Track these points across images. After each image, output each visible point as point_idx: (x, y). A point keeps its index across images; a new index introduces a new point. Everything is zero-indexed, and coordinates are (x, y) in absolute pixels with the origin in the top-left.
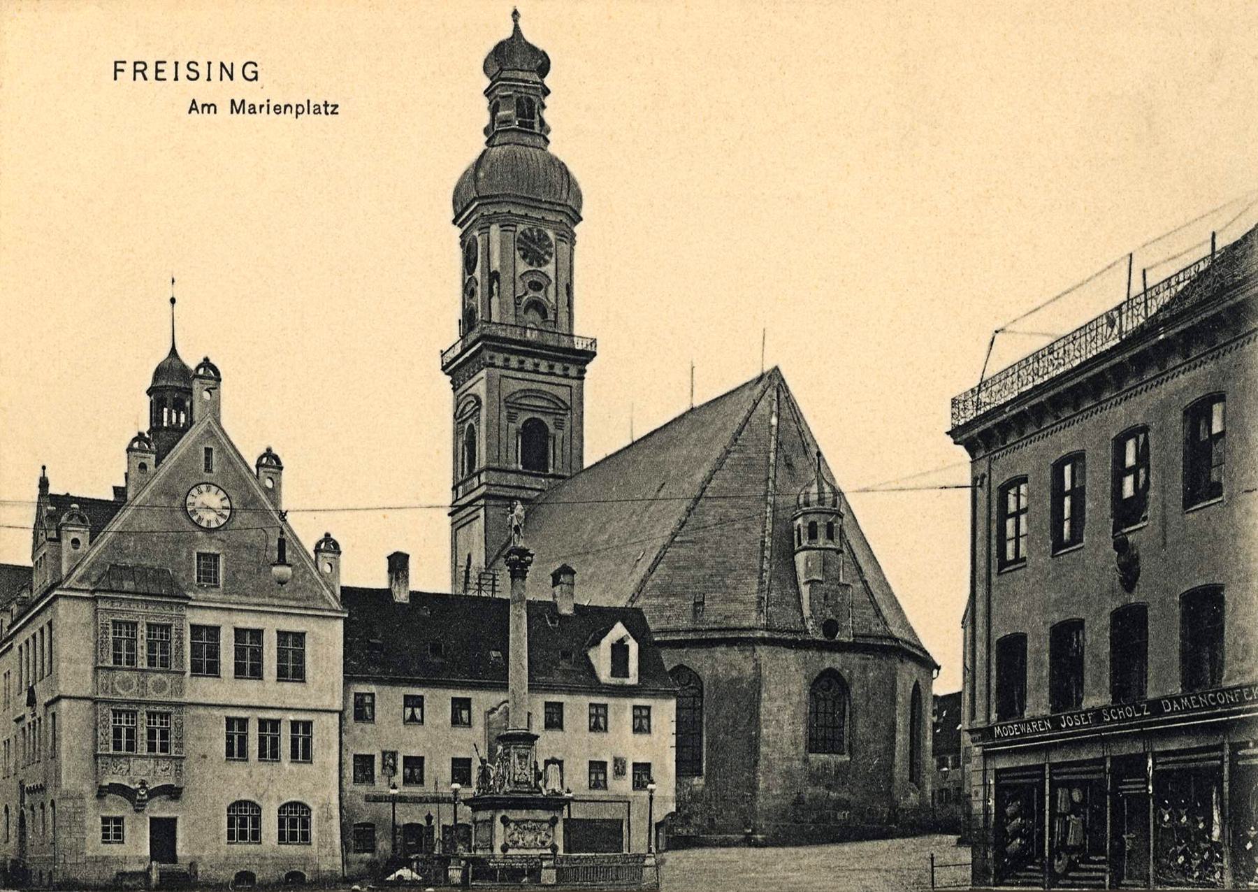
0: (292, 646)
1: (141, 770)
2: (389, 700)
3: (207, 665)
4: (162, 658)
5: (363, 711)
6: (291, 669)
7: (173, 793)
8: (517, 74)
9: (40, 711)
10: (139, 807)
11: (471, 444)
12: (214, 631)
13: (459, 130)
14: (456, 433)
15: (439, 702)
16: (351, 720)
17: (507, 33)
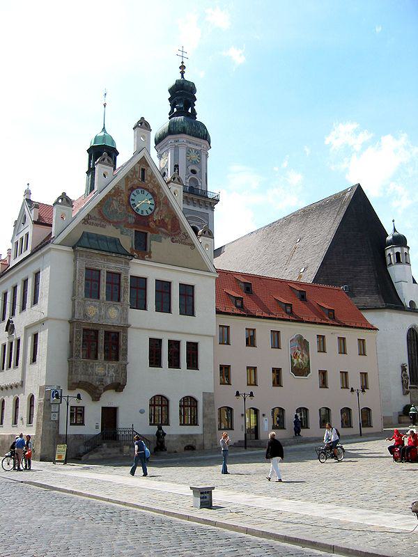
0: (187, 292)
1: (102, 369)
2: (238, 327)
3: (140, 304)
4: (114, 295)
6: (188, 308)
7: (119, 387)
8: (183, 96)
9: (19, 333)
10: (96, 398)
15: (264, 329)
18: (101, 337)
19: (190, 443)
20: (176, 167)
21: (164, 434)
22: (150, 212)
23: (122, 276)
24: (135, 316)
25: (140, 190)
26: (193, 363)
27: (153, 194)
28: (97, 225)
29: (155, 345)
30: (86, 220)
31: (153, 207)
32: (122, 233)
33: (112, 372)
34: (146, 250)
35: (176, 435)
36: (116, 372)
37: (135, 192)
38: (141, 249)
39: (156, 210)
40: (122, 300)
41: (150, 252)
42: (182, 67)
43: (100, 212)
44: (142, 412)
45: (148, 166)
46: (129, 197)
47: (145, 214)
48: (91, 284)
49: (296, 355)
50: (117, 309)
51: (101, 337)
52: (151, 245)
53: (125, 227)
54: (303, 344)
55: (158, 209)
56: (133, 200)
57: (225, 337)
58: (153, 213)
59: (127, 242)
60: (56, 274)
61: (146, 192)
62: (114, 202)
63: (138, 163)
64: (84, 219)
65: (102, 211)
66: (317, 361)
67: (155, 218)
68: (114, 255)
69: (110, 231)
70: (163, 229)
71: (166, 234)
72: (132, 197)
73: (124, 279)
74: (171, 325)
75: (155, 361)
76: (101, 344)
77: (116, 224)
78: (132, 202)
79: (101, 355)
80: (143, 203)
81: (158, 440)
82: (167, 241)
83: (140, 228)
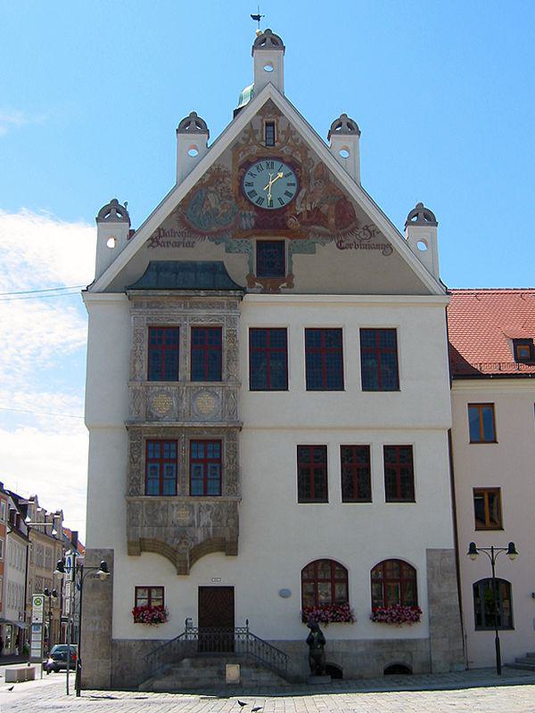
7: (229, 546)
10: (183, 570)
18: (184, 452)
19: (399, 658)
21: (323, 642)
22: (287, 200)
23: (224, 333)
24: (259, 407)
25: (263, 164)
26: (401, 486)
27: (294, 166)
28: (177, 245)
30: (154, 241)
31: (293, 190)
32: (228, 250)
33: (206, 518)
34: (283, 273)
35: (366, 642)
36: (216, 517)
37: (253, 170)
38: (272, 271)
39: (301, 194)
40: (224, 376)
41: (291, 276)
43: (182, 221)
44: (285, 594)
45: (280, 114)
46: (241, 179)
47: (277, 205)
48: (159, 356)
50: (214, 394)
51: (184, 452)
52: (291, 263)
53: (234, 236)
55: (304, 190)
56: (250, 184)
58: (295, 199)
59: (240, 264)
61: (277, 164)
62: (210, 196)
63: (258, 113)
64: (151, 238)
65: (189, 215)
67: (300, 209)
68: (202, 293)
69: (204, 251)
70: (317, 228)
71: (326, 235)
72: (248, 179)
73: (228, 336)
75: (311, 486)
76: (184, 465)
77: (216, 237)
78: (247, 189)
79: (184, 486)
80: (272, 185)
81: (311, 655)
82: (328, 250)
83: (266, 235)
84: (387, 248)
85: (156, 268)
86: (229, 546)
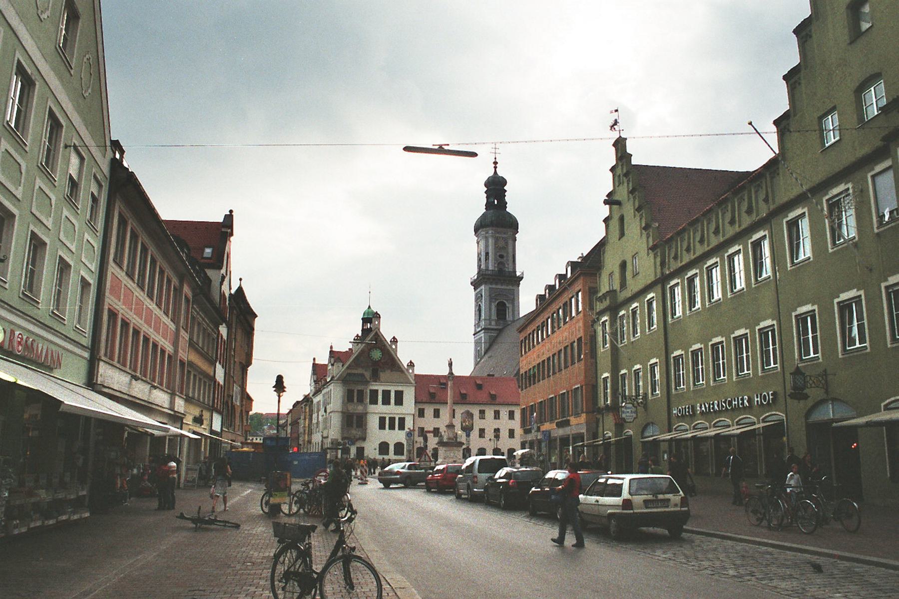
1: (355, 432)
3: (374, 401)
5: (421, 413)
6: (399, 401)
11: (480, 310)
12: (377, 391)
13: (478, 206)
14: (476, 306)
16: (417, 417)
17: (491, 173)
20: (487, 254)
24: (372, 408)
27: (382, 350)
29: (382, 421)
38: (376, 377)
42: (495, 163)
49: (465, 421)
54: (470, 415)
57: (421, 413)
59: (368, 375)
60: (335, 393)
66: (478, 424)
69: (360, 371)
74: (391, 410)
75: (382, 426)
76: (355, 422)
79: (355, 425)
80: (377, 355)
82: (388, 372)
84: (402, 372)
85: (349, 375)
86: (364, 439)
